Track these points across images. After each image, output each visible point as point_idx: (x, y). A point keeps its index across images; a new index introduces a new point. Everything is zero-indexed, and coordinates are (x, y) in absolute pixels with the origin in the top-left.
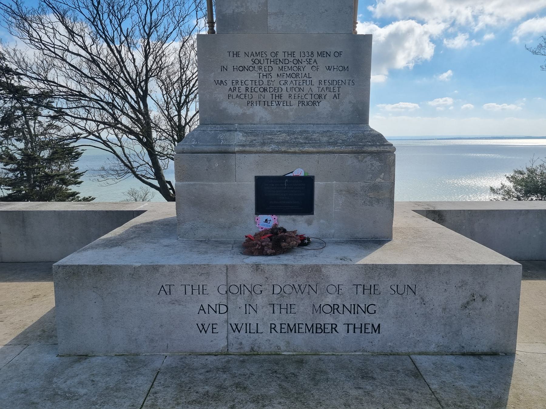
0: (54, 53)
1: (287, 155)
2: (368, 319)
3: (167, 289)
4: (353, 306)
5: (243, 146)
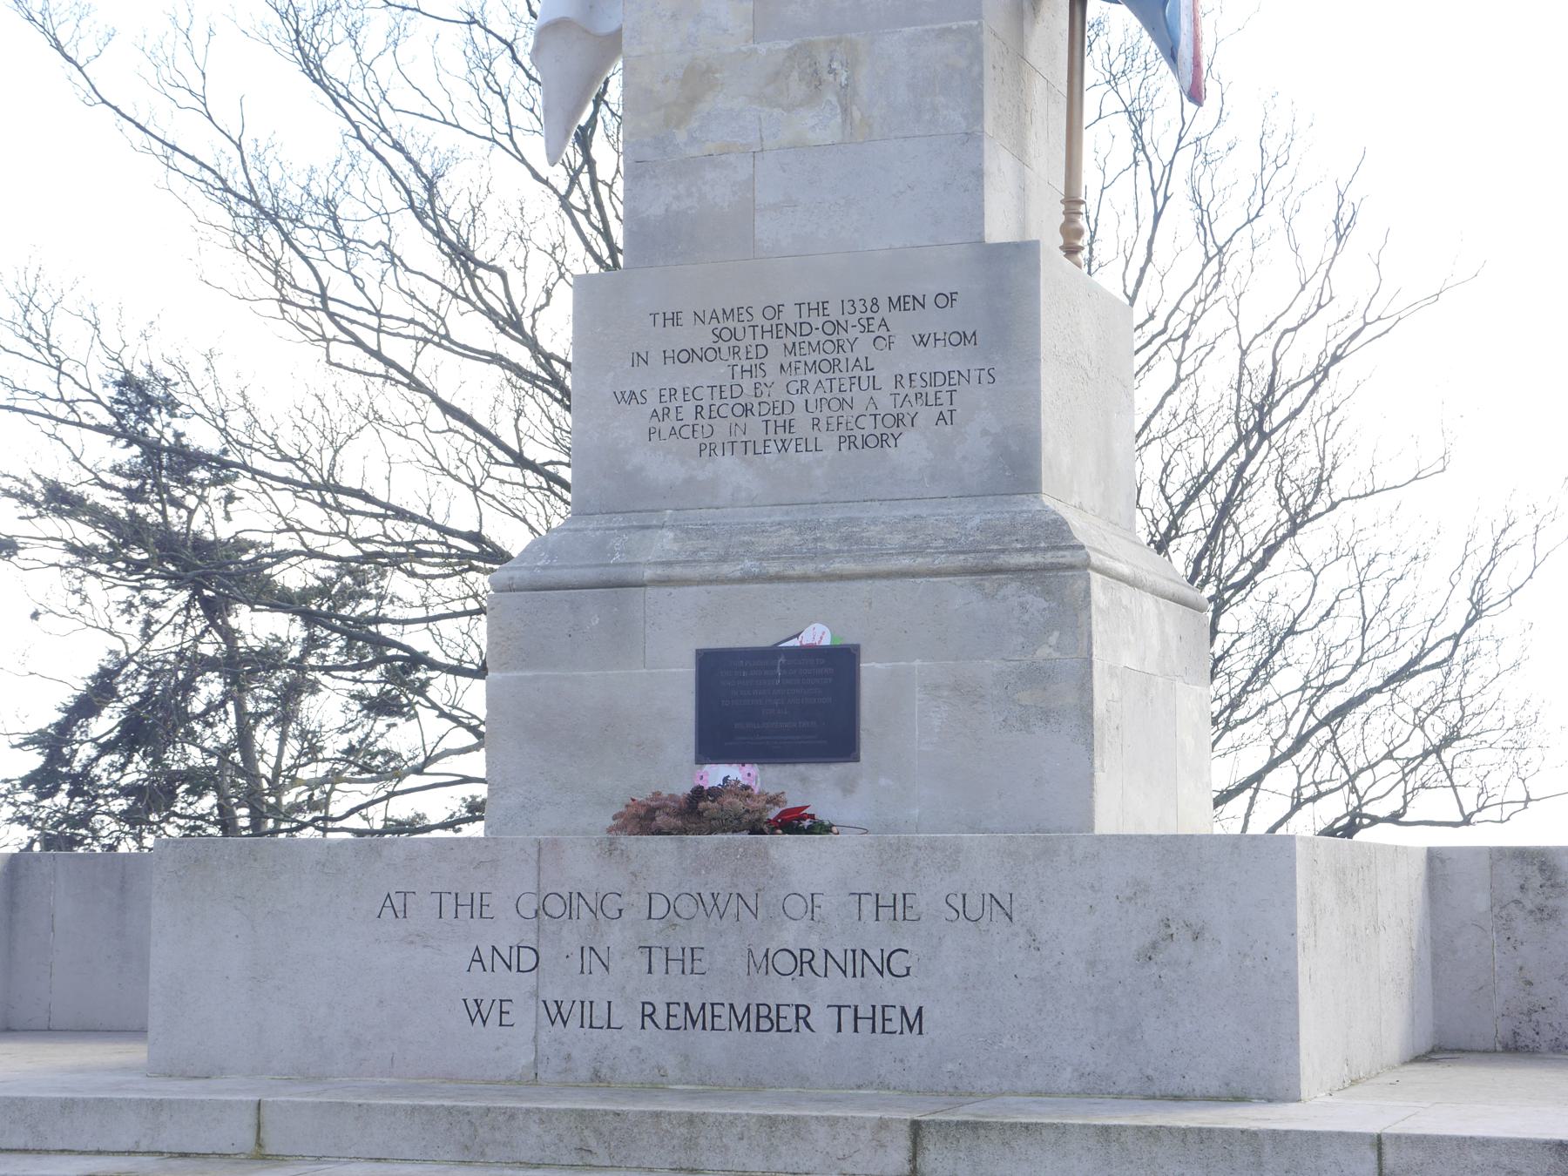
0: (377, 354)
1: (782, 586)
2: (890, 991)
3: (398, 901)
4: (850, 954)
5: (669, 564)
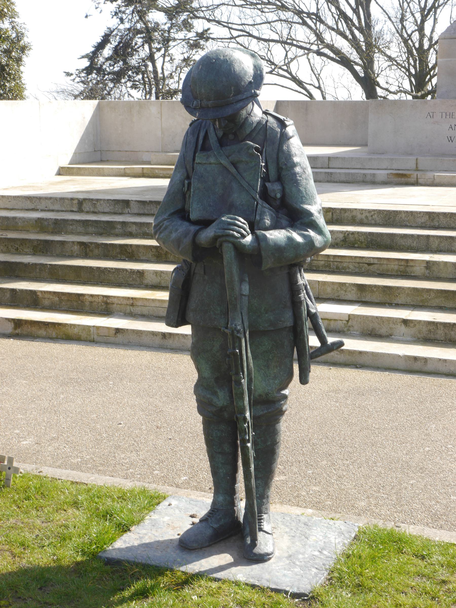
3: (431, 114)
